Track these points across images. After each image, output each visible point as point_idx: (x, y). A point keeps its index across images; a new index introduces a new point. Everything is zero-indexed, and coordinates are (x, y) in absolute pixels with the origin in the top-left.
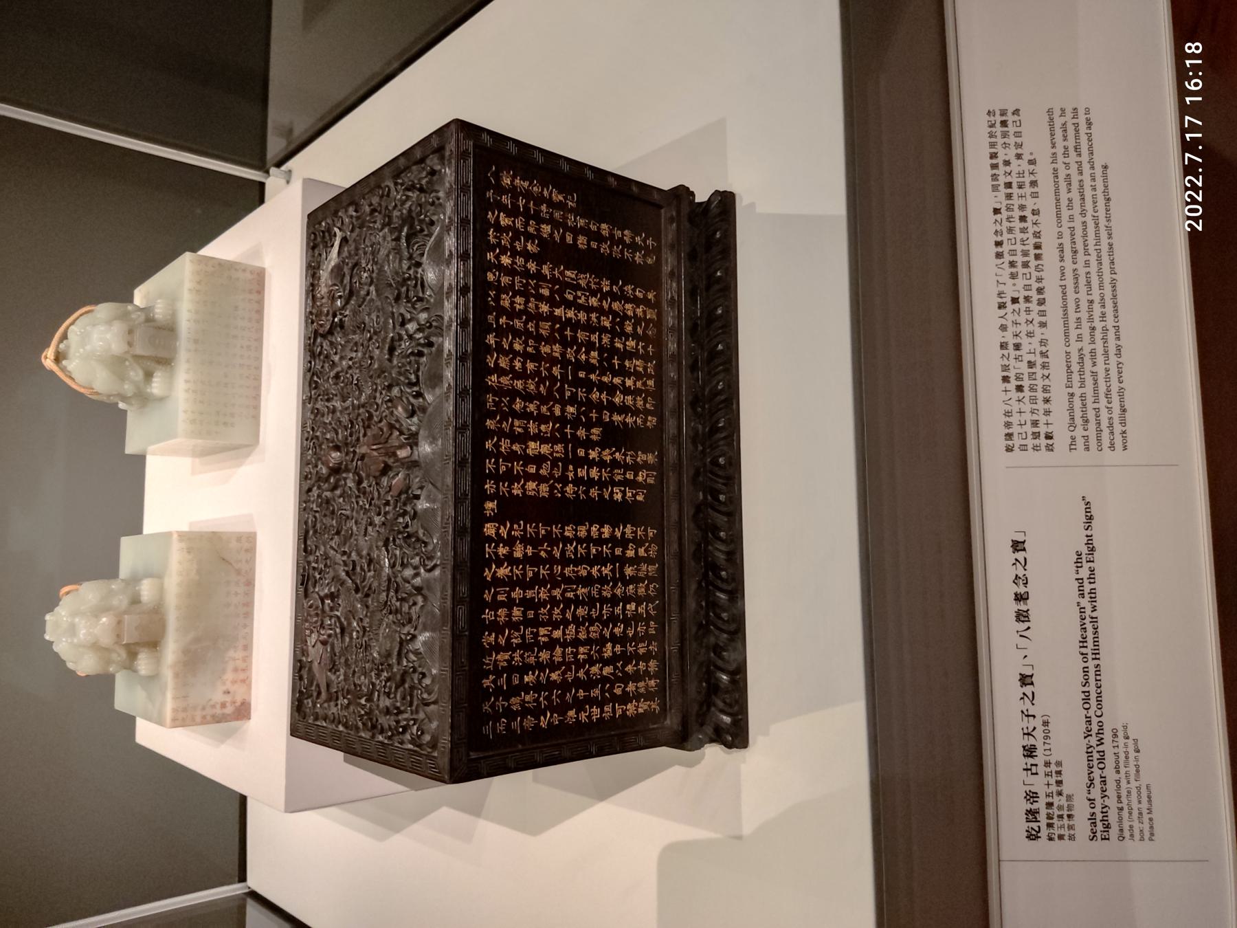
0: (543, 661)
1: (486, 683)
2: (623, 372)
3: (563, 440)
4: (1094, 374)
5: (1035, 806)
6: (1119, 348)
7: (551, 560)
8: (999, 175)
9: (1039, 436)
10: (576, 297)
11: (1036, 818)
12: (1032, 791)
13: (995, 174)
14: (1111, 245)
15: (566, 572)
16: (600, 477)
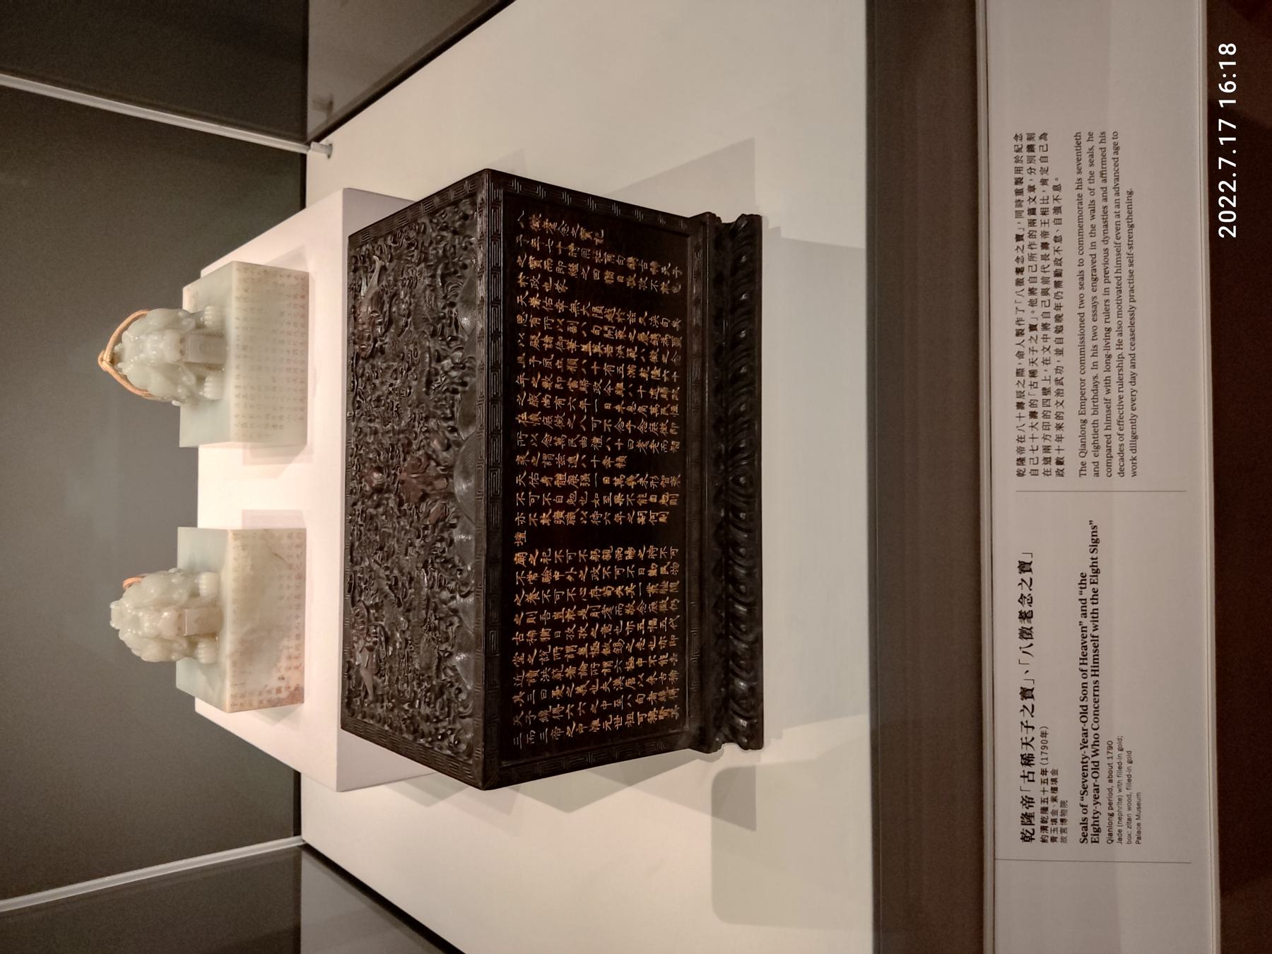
0: (569, 676)
1: (517, 698)
2: (648, 400)
3: (590, 469)
4: (1108, 401)
5: (1030, 811)
6: (1133, 376)
7: (577, 583)
8: (1023, 201)
9: (1050, 461)
10: (603, 332)
11: (1030, 821)
12: (1029, 796)
13: (1019, 201)
14: (1131, 273)
15: (591, 593)
16: (625, 502)
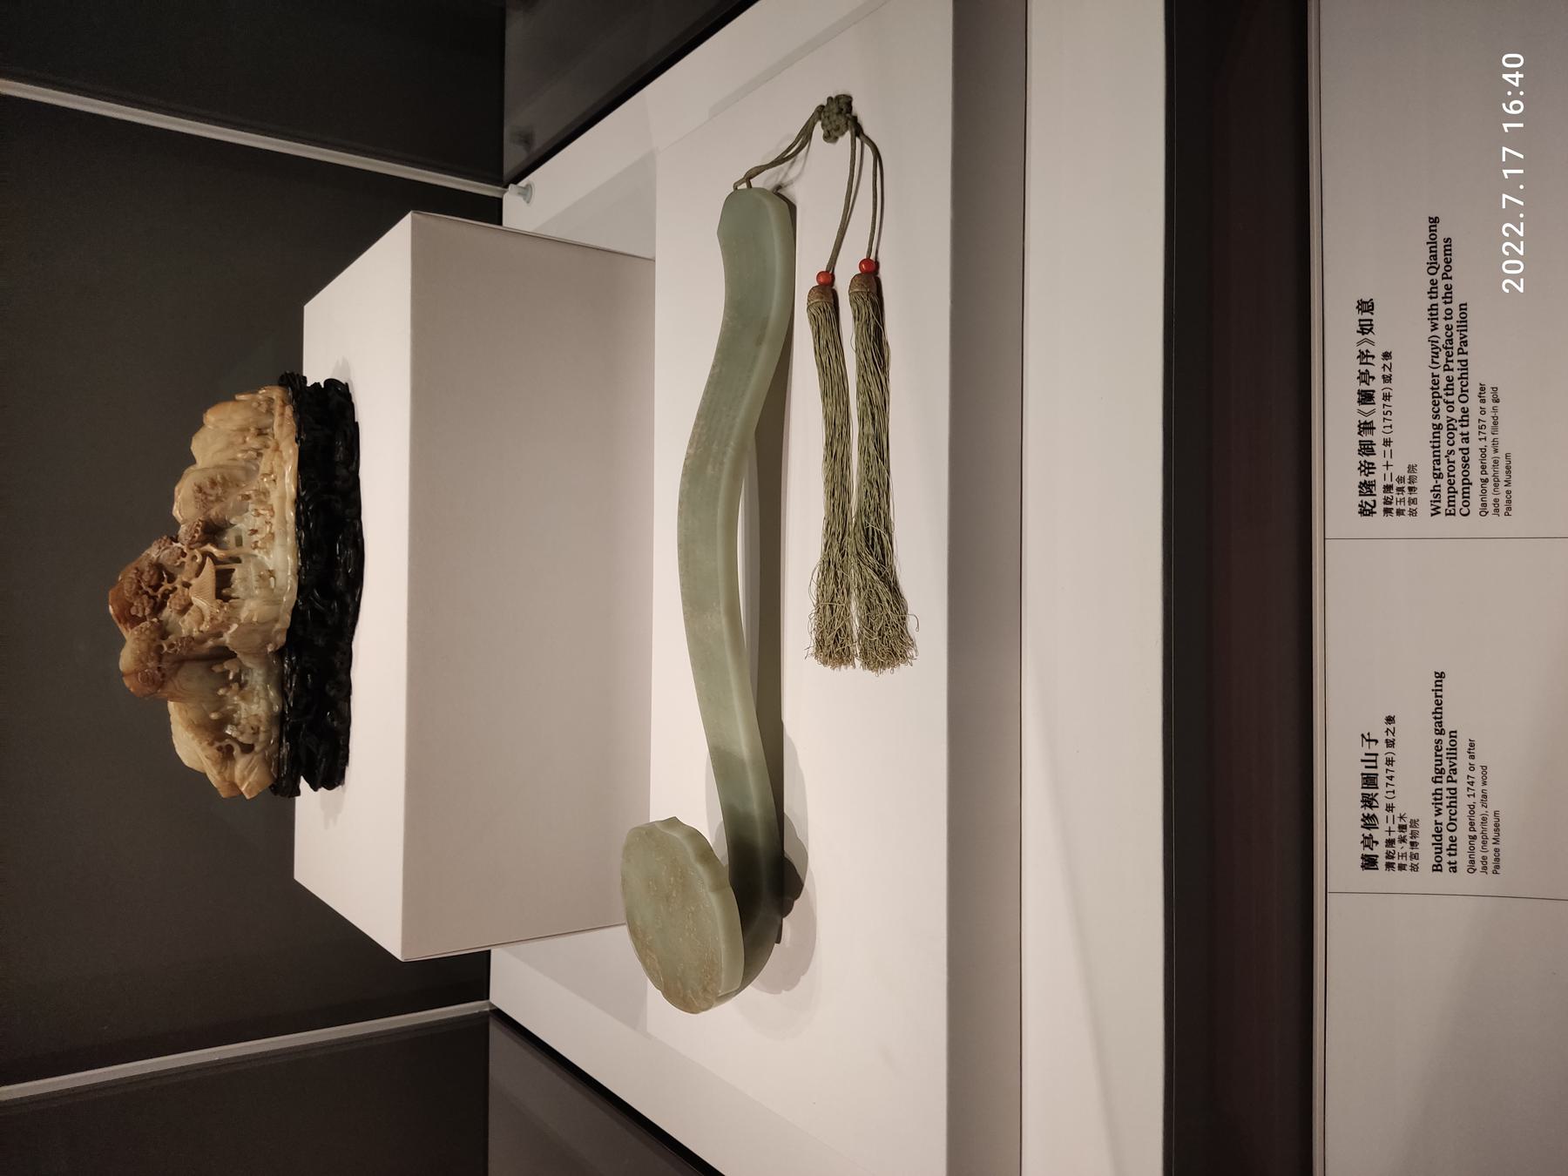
11: (1371, 491)
12: (1368, 461)
